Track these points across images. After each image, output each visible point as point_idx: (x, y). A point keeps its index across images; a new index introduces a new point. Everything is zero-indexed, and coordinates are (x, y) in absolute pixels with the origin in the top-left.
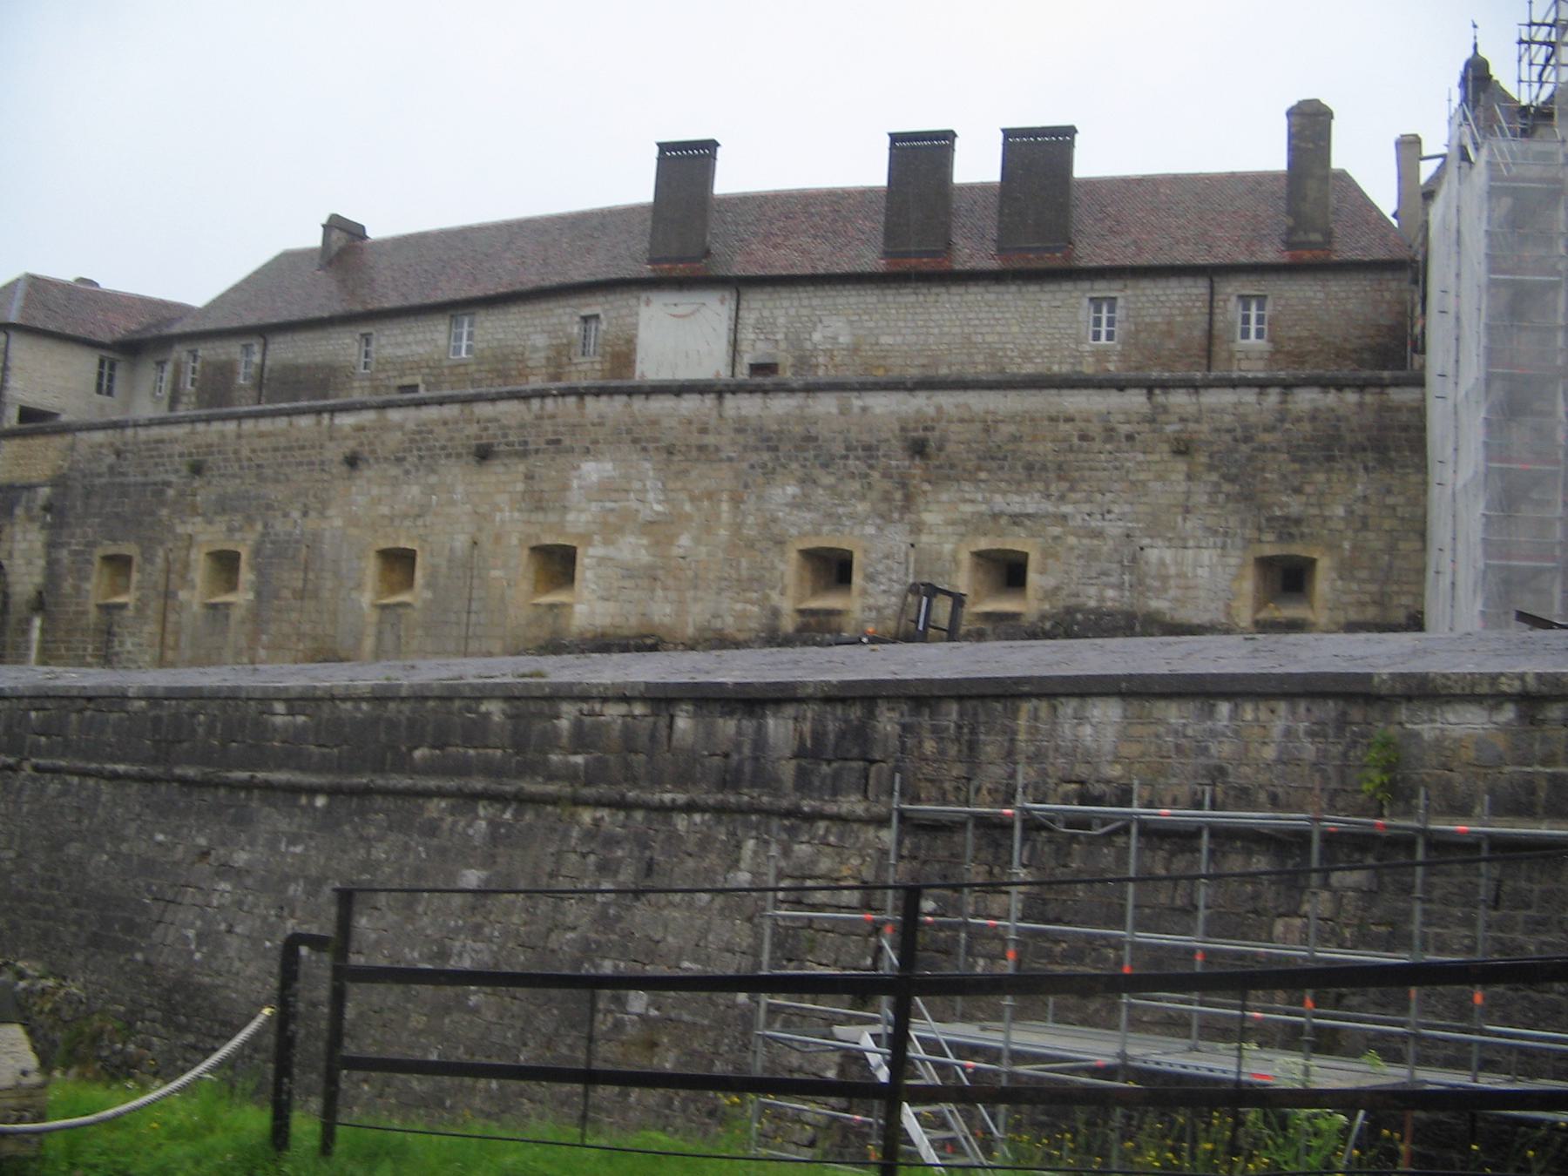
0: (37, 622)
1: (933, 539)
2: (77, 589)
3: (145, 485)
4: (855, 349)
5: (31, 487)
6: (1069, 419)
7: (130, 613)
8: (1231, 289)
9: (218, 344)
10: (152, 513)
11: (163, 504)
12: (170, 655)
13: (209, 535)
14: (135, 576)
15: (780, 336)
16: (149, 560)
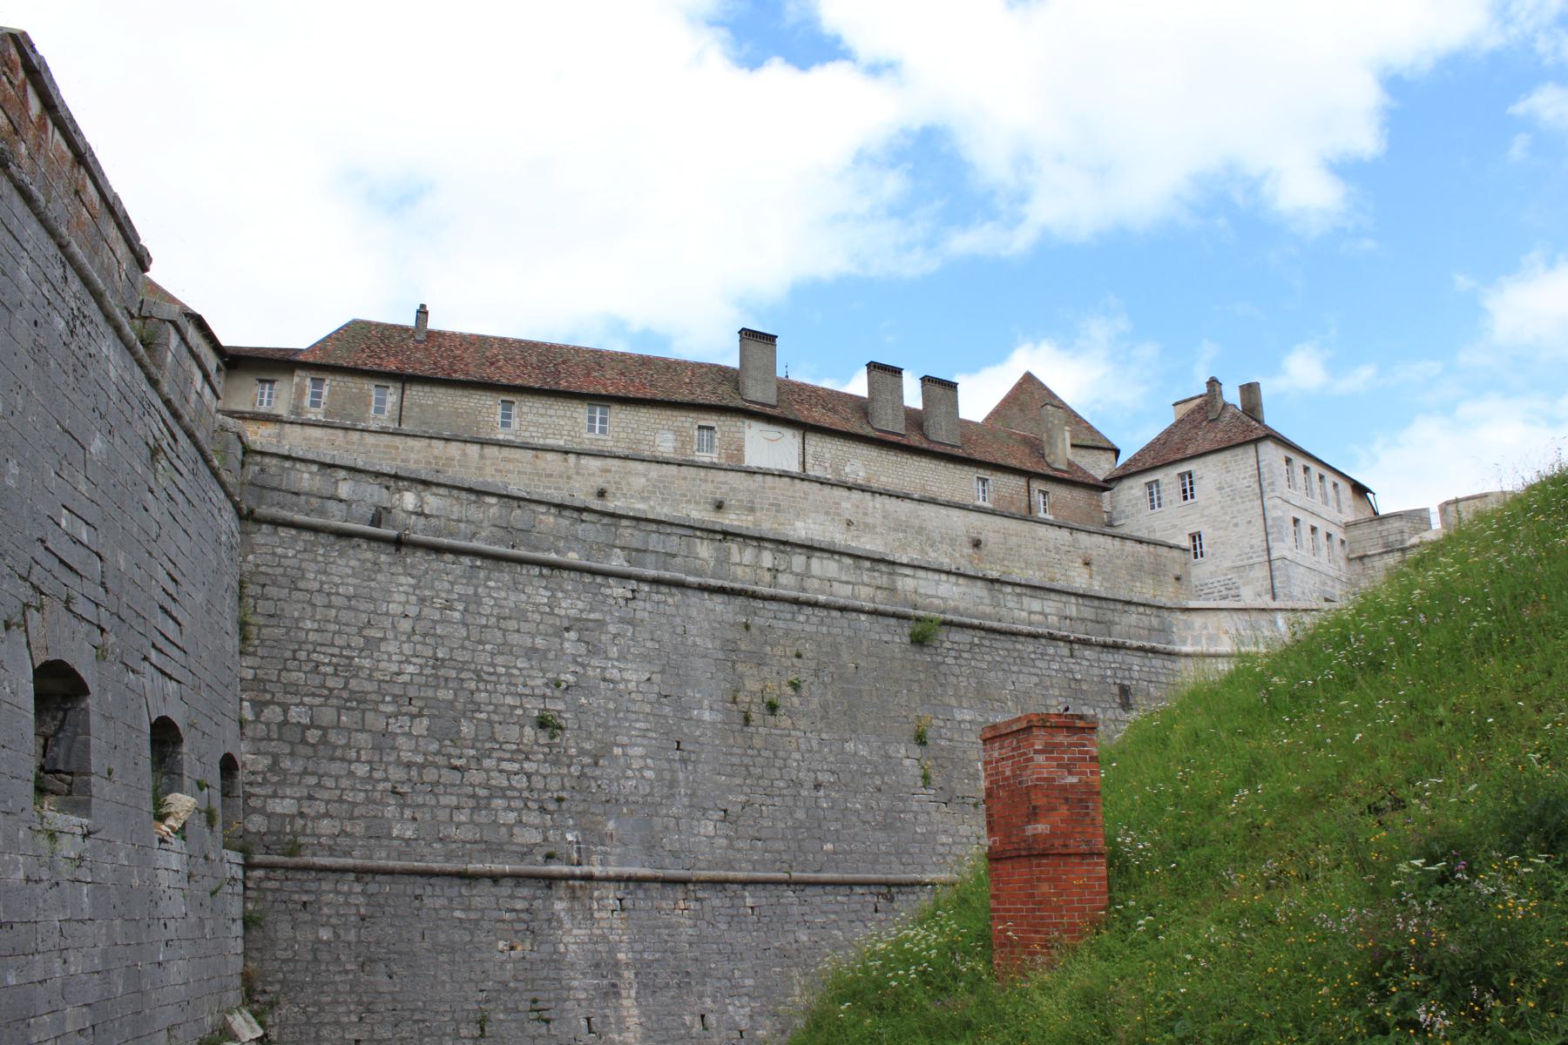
8: (1036, 485)
9: (347, 379)
15: (827, 465)
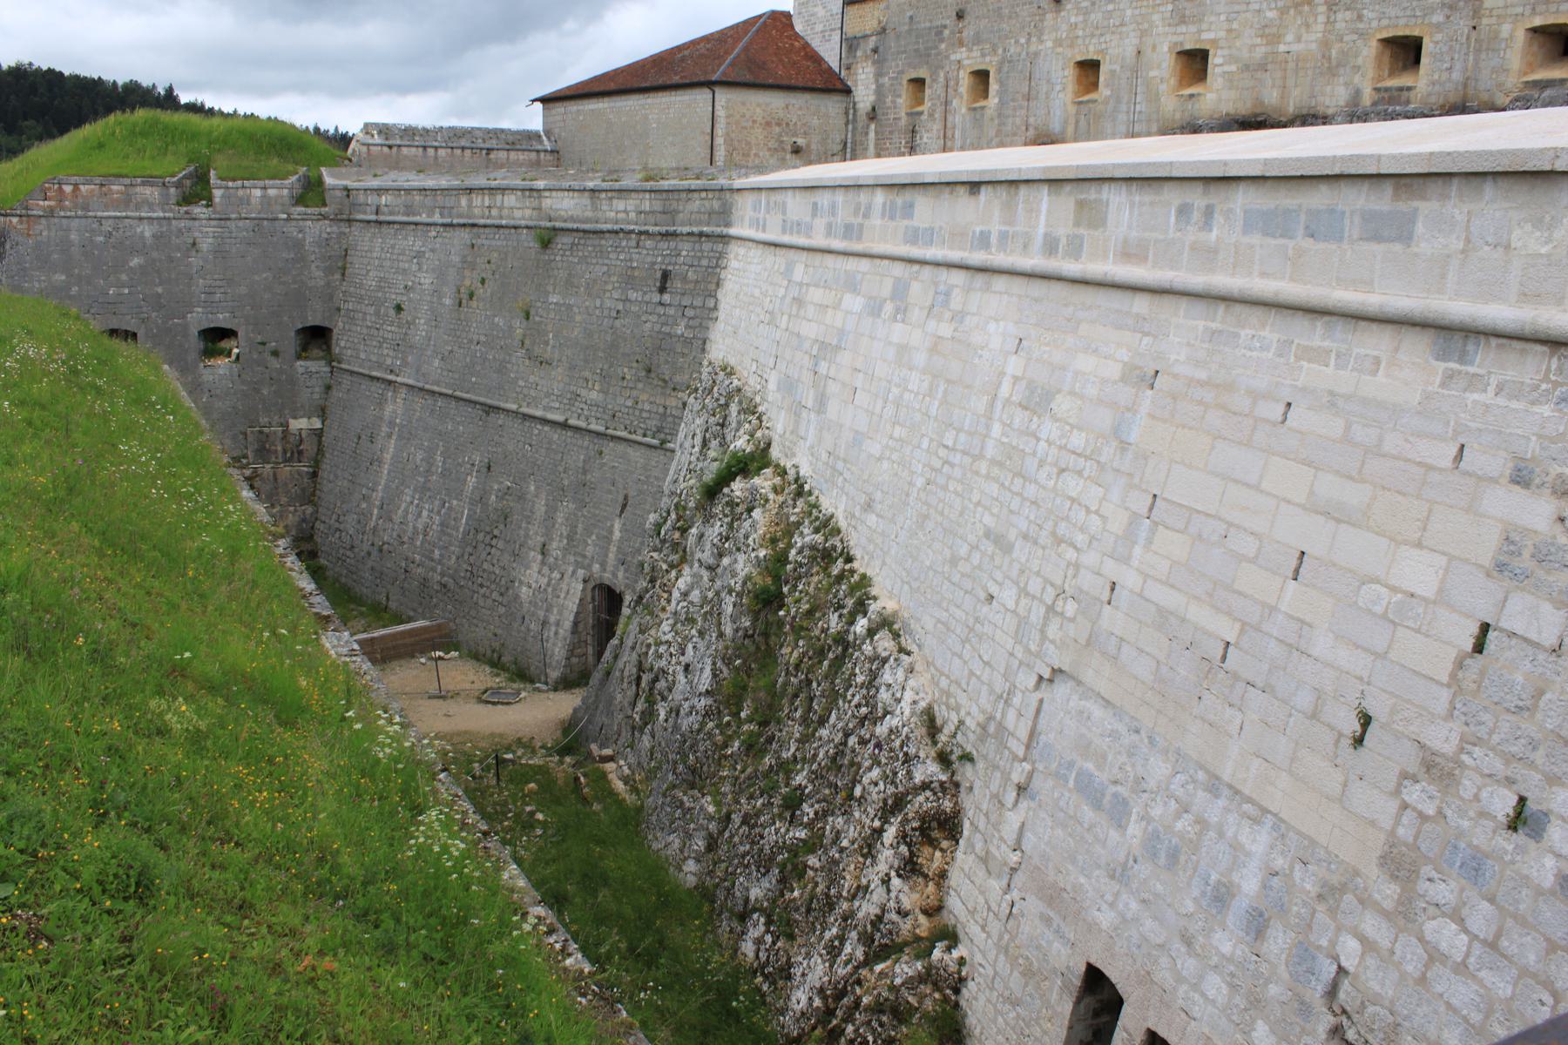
0: (873, 126)
1: (1494, 20)
2: (893, 102)
3: (930, 28)
5: (865, 37)
7: (925, 117)
10: (936, 47)
11: (942, 40)
12: (949, 144)
13: (971, 59)
14: (928, 91)
16: (934, 80)
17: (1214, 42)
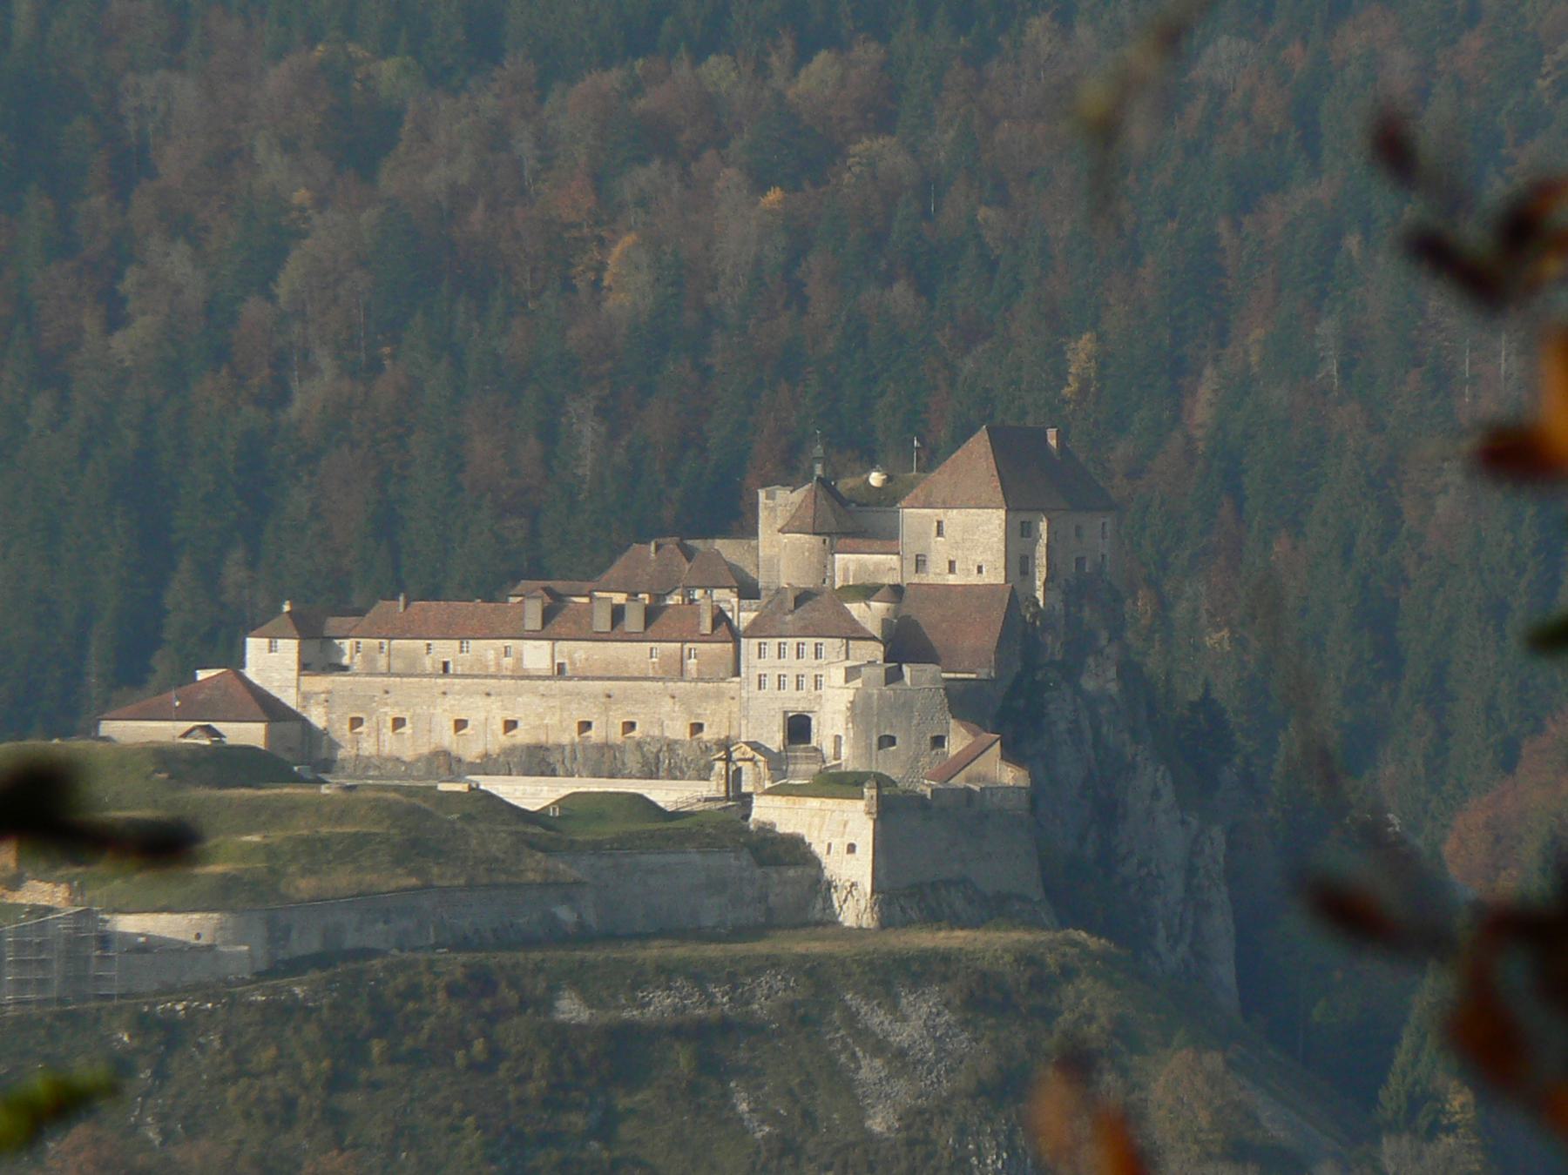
4: (587, 659)
6: (645, 689)
7: (364, 736)
13: (397, 712)
17: (520, 718)
